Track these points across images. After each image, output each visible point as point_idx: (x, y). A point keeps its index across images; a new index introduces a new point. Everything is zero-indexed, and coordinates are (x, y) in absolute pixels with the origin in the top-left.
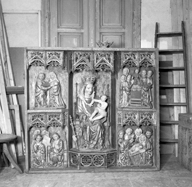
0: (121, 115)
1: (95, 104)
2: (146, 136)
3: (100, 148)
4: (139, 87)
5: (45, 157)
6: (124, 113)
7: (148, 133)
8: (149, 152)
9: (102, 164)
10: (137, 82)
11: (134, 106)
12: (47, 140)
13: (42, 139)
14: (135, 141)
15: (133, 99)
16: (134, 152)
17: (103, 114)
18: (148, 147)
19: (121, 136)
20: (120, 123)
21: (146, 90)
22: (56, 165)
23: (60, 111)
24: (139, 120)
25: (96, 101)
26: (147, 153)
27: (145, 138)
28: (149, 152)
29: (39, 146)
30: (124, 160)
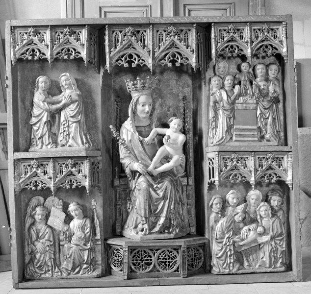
0: (216, 161)
1: (160, 141)
2: (272, 207)
3: (174, 232)
5: (55, 255)
6: (222, 157)
7: (275, 200)
8: (278, 242)
9: (175, 268)
10: (246, 90)
11: (241, 141)
12: (57, 219)
13: (47, 217)
14: (250, 219)
15: (238, 127)
16: (245, 242)
17: (177, 159)
18: (275, 230)
19: (216, 208)
20: (212, 179)
21: (267, 107)
22: (77, 270)
24: (256, 170)
25: (161, 131)
26: (273, 243)
27: (270, 211)
28: (278, 242)
29: (40, 230)
30: (223, 258)
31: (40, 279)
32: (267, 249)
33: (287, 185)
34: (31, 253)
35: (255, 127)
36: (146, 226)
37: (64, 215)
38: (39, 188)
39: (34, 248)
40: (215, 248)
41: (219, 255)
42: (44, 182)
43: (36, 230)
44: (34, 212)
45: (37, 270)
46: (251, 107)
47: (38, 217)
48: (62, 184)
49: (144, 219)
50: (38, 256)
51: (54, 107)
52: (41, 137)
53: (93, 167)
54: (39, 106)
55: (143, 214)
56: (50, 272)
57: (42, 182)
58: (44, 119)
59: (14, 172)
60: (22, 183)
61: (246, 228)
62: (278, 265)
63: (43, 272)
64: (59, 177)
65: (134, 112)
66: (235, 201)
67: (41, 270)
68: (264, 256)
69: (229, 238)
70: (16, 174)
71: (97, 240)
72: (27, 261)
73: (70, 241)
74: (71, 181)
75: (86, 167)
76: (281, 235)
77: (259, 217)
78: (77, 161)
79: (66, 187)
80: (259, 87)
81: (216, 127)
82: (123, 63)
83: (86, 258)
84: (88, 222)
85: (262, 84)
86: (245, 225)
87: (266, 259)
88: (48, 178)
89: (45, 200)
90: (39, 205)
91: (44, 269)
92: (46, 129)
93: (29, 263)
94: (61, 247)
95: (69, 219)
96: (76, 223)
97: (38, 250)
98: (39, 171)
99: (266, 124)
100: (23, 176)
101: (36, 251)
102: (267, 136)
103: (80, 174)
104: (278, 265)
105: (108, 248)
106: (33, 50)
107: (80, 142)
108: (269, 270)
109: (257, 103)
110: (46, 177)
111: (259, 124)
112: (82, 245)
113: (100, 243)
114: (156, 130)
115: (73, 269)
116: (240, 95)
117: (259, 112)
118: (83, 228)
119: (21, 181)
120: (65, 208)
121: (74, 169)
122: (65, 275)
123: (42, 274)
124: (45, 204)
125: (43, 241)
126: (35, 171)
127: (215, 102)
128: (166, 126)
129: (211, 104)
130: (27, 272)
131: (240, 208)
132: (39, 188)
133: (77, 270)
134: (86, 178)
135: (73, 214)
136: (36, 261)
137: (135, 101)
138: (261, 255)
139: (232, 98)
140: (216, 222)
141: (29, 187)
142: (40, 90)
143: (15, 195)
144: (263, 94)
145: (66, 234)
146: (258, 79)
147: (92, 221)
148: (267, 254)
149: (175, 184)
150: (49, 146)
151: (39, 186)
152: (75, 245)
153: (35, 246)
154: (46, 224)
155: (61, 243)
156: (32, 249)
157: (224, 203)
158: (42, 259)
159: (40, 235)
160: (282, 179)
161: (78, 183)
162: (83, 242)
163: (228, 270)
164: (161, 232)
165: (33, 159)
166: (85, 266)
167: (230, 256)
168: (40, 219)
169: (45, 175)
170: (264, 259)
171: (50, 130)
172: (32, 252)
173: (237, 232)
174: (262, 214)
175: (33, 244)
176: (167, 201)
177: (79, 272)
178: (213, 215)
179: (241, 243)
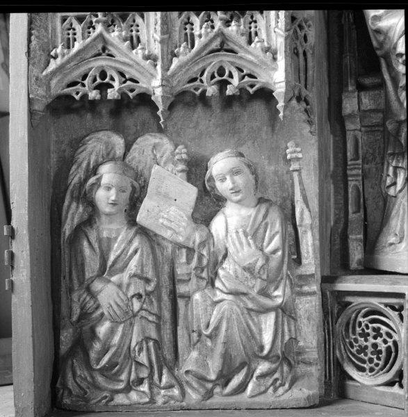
5: (159, 328)
12: (169, 207)
29: (110, 241)
34: (79, 319)
37: (192, 192)
38: (112, 94)
39: (91, 304)
42: (130, 72)
43: (100, 240)
44: (92, 180)
45: (100, 379)
47: (104, 198)
48: (194, 80)
50: (102, 330)
56: (145, 387)
57: (122, 74)
59: (30, 35)
60: (54, 73)
63: (121, 386)
64: (185, 54)
67: (115, 378)
70: (34, 43)
71: (305, 278)
72: (64, 348)
73: (211, 283)
74: (221, 71)
79: (204, 92)
83: (267, 338)
84: (276, 223)
88: (147, 58)
89: (128, 147)
90: (109, 157)
91: (124, 377)
93: (72, 352)
94: (181, 303)
95: (208, 204)
96: (230, 223)
97: (104, 309)
98: (116, 33)
100: (59, 50)
101: (98, 312)
105: (335, 307)
110: (138, 54)
112: (254, 293)
113: (315, 287)
115: (224, 378)
118: (256, 234)
119: (53, 65)
120: (196, 170)
122: (193, 396)
123: (118, 392)
124: (129, 158)
125: (125, 277)
126: (101, 35)
130: (65, 386)
132: (112, 94)
133: (236, 381)
134: (275, 59)
135: (224, 187)
136: (97, 346)
141: (76, 93)
143: (31, 113)
145: (201, 257)
147: (290, 218)
151: (112, 86)
152: (230, 293)
153: (93, 296)
154: (132, 222)
155: (182, 289)
156: (82, 308)
158: (116, 339)
159: (112, 258)
161: (247, 79)
162: (258, 285)
166: (263, 367)
168: (114, 204)
169: (133, 47)
172: (85, 315)
175: (88, 289)
177: (242, 388)
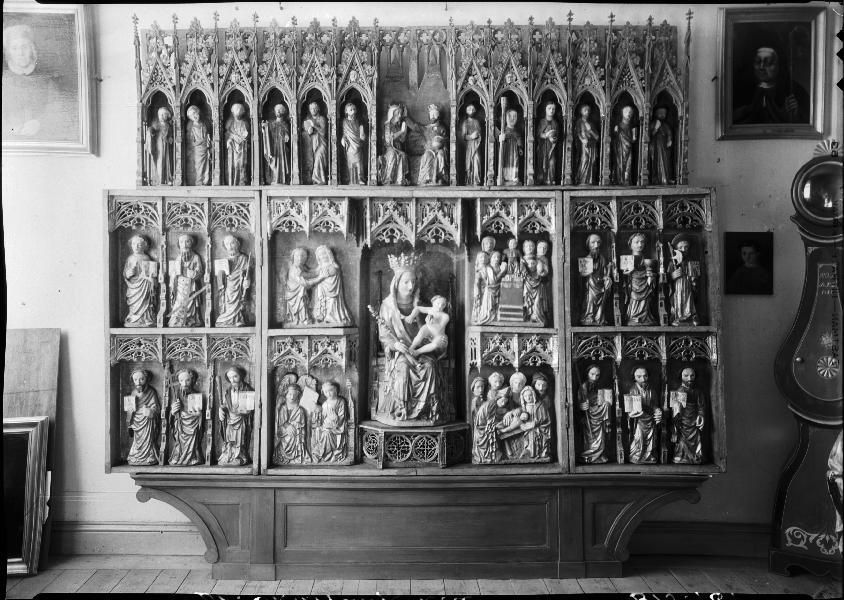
4: (517, 279)
7: (540, 385)
9: (433, 457)
12: (309, 398)
14: (512, 403)
19: (478, 391)
22: (329, 456)
23: (341, 332)
25: (424, 309)
26: (538, 431)
29: (291, 411)
31: (289, 466)
32: (531, 436)
33: (552, 369)
35: (521, 307)
36: (404, 411)
40: (477, 435)
41: (481, 443)
46: (518, 286)
49: (402, 403)
51: (311, 282)
52: (298, 313)
53: (350, 344)
54: (294, 280)
55: (402, 397)
58: (301, 294)
61: (508, 414)
62: (543, 454)
64: (315, 356)
65: (396, 291)
66: (498, 385)
68: (529, 445)
69: (491, 424)
73: (322, 424)
75: (342, 345)
76: (546, 422)
77: (522, 402)
78: (332, 340)
80: (526, 265)
81: (481, 303)
82: (384, 238)
83: (338, 443)
84: (342, 403)
85: (530, 263)
86: (509, 410)
87: (531, 448)
92: (302, 304)
96: (329, 405)
99: (533, 304)
102: (534, 317)
103: (337, 353)
104: (543, 454)
105: (360, 433)
106: (290, 223)
107: (337, 317)
108: (533, 460)
109: (524, 282)
111: (526, 304)
114: (417, 309)
115: (324, 455)
116: (506, 273)
117: (525, 291)
118: (336, 410)
121: (330, 348)
122: (315, 461)
127: (481, 280)
128: (429, 304)
129: (477, 281)
131: (503, 392)
133: (329, 456)
135: (327, 395)
137: (398, 277)
138: (526, 443)
139: (498, 276)
140: (478, 406)
142: (295, 264)
144: (531, 272)
146: (526, 257)
147: (346, 403)
148: (531, 442)
149: (436, 366)
150: (306, 323)
155: (313, 426)
157: (486, 386)
160: (548, 362)
163: (489, 461)
164: (418, 418)
165: (287, 336)
166: (336, 452)
167: (492, 444)
170: (529, 448)
171: (306, 306)
173: (500, 418)
174: (527, 399)
176: (428, 385)
177: (330, 459)
178: (475, 400)
179: (504, 431)
